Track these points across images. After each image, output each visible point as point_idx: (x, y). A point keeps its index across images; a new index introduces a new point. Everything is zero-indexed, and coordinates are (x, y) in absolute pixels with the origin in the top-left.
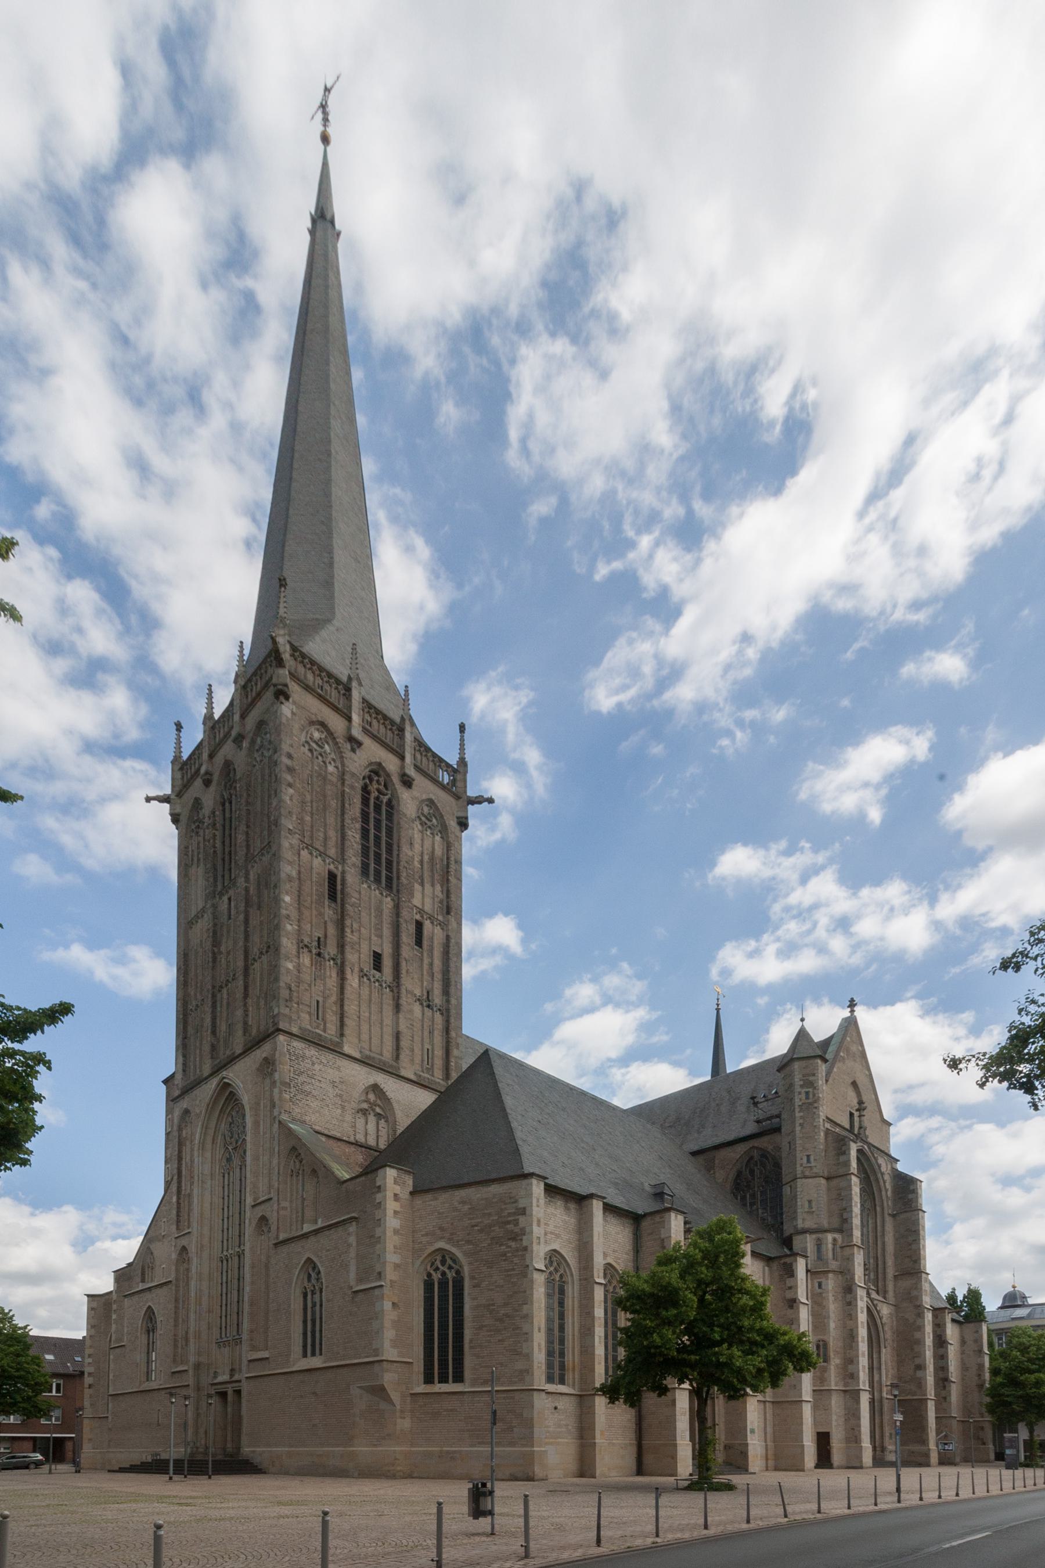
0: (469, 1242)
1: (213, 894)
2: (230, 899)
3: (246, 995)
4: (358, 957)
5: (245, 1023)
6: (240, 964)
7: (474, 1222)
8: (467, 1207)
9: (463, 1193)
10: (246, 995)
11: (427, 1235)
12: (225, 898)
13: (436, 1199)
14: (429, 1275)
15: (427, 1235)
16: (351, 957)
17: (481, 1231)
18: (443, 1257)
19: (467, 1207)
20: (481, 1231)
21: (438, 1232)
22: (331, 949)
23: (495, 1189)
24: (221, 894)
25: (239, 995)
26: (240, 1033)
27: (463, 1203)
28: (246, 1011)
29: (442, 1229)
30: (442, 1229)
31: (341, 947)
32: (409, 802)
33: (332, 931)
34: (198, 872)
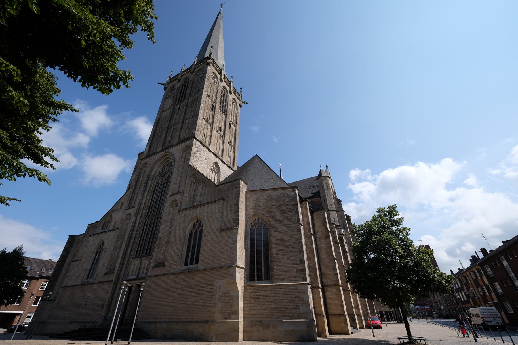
0: (271, 212)
1: (174, 105)
2: (180, 106)
3: (181, 128)
4: (216, 126)
5: (180, 136)
6: (181, 120)
7: (273, 204)
8: (270, 198)
9: (268, 192)
10: (181, 128)
11: (252, 208)
12: (178, 106)
13: (256, 194)
14: (252, 226)
15: (252, 208)
16: (215, 125)
17: (276, 208)
18: (259, 218)
19: (270, 198)
20: (276, 208)
21: (258, 207)
22: (210, 121)
23: (281, 192)
24: (177, 105)
25: (179, 128)
26: (177, 138)
27: (268, 196)
28: (180, 133)
29: (259, 206)
30: (259, 206)
31: (213, 122)
32: (231, 97)
33: (211, 117)
34: (170, 102)
